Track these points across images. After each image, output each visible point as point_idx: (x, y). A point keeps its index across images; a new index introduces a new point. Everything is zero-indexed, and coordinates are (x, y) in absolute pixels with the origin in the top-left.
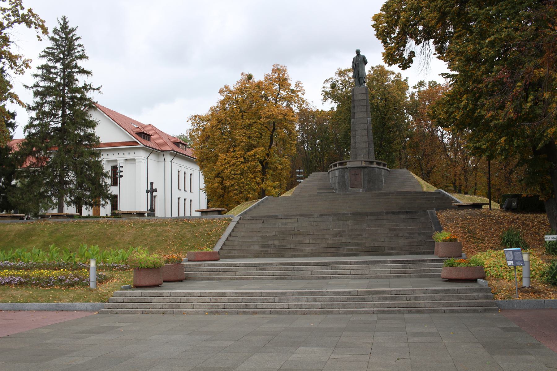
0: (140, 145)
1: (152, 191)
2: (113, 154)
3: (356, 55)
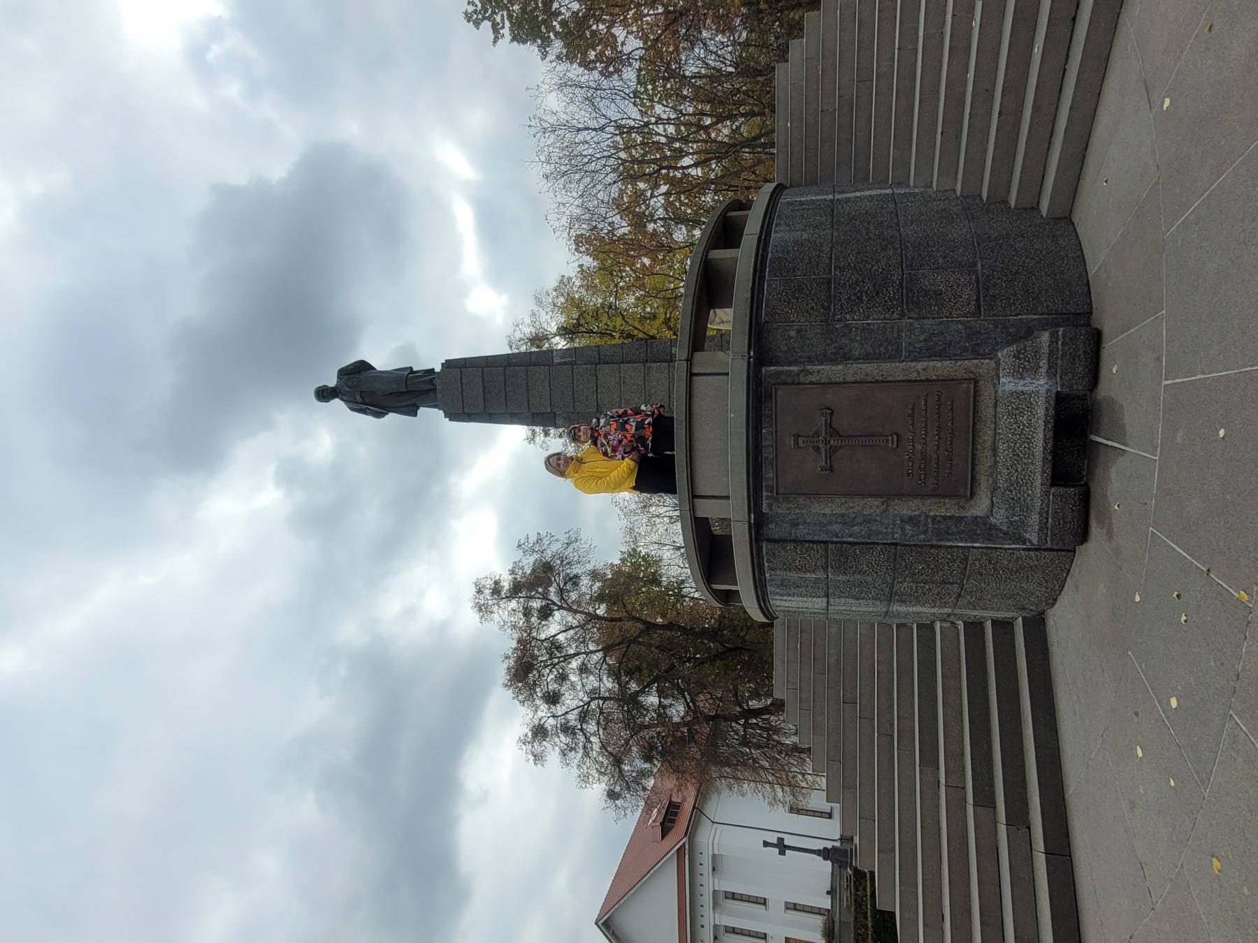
0: (684, 843)
1: (782, 847)
2: (702, 895)
3: (337, 403)
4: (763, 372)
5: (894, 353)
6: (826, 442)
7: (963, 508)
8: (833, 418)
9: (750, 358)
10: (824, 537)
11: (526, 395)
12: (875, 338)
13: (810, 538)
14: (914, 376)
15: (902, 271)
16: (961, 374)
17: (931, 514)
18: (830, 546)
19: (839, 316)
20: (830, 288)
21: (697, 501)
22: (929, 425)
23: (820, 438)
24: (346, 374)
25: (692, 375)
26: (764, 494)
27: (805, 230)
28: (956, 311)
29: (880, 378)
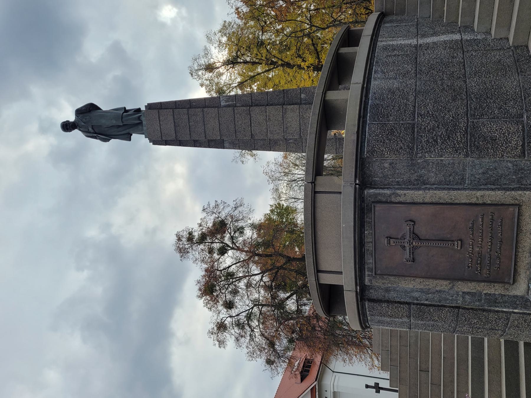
0: (315, 385)
3: (77, 132)
4: (366, 193)
5: (459, 181)
6: (410, 243)
7: (507, 289)
8: (415, 227)
9: (356, 184)
10: (408, 300)
11: (203, 128)
12: (447, 170)
13: (399, 300)
14: (474, 200)
15: (468, 119)
16: (509, 201)
17: (485, 292)
18: (412, 306)
19: (420, 155)
20: (413, 132)
21: (320, 274)
22: (484, 235)
23: (406, 240)
24: (82, 113)
25: (315, 192)
26: (367, 273)
27: (395, 79)
28: (507, 154)
29: (450, 201)
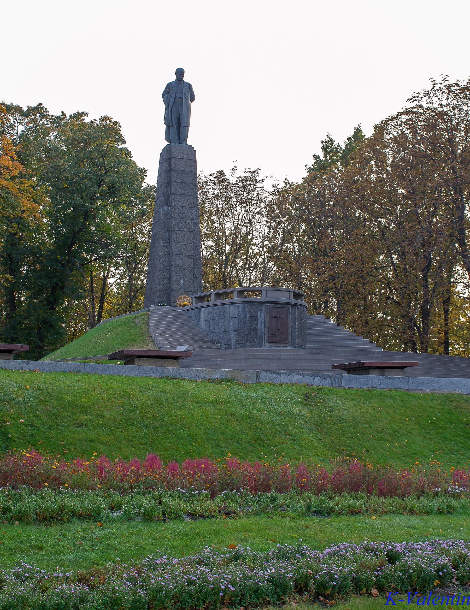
3: (173, 78)
